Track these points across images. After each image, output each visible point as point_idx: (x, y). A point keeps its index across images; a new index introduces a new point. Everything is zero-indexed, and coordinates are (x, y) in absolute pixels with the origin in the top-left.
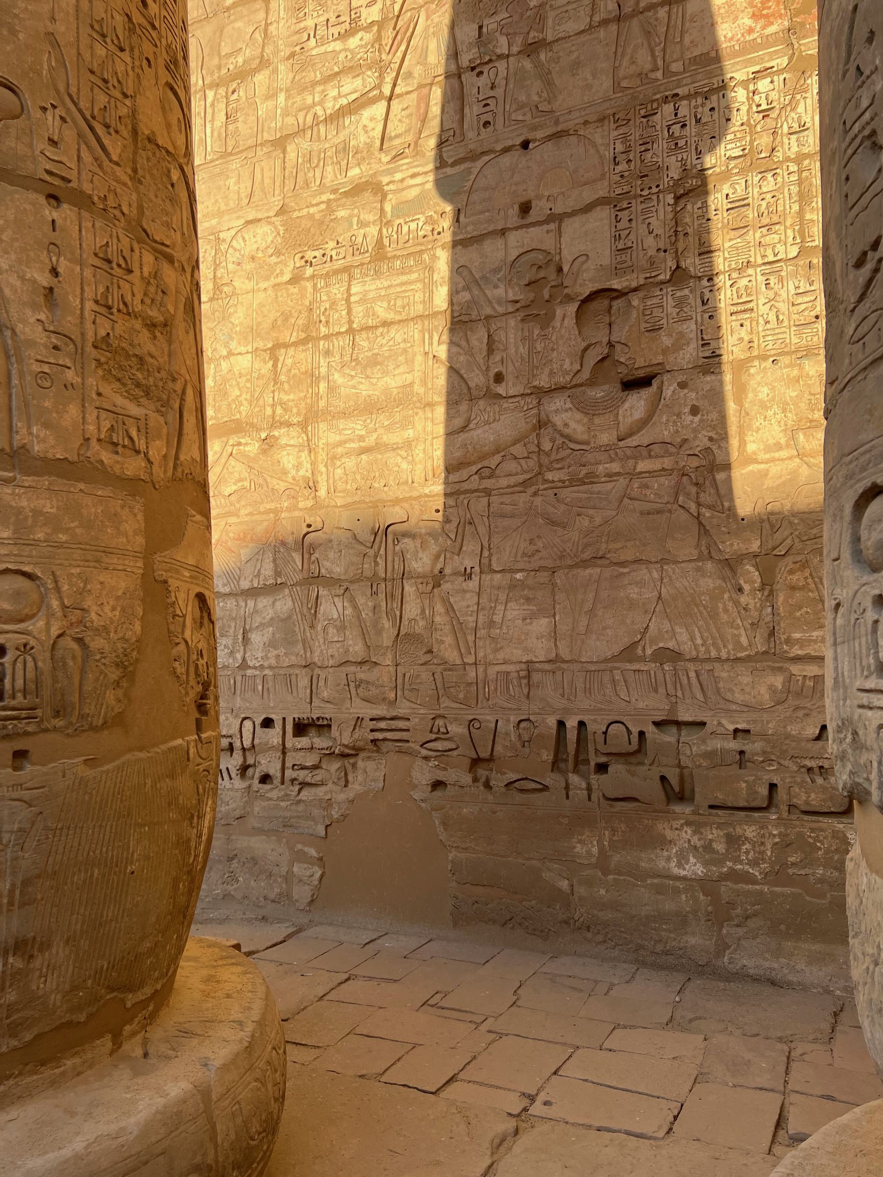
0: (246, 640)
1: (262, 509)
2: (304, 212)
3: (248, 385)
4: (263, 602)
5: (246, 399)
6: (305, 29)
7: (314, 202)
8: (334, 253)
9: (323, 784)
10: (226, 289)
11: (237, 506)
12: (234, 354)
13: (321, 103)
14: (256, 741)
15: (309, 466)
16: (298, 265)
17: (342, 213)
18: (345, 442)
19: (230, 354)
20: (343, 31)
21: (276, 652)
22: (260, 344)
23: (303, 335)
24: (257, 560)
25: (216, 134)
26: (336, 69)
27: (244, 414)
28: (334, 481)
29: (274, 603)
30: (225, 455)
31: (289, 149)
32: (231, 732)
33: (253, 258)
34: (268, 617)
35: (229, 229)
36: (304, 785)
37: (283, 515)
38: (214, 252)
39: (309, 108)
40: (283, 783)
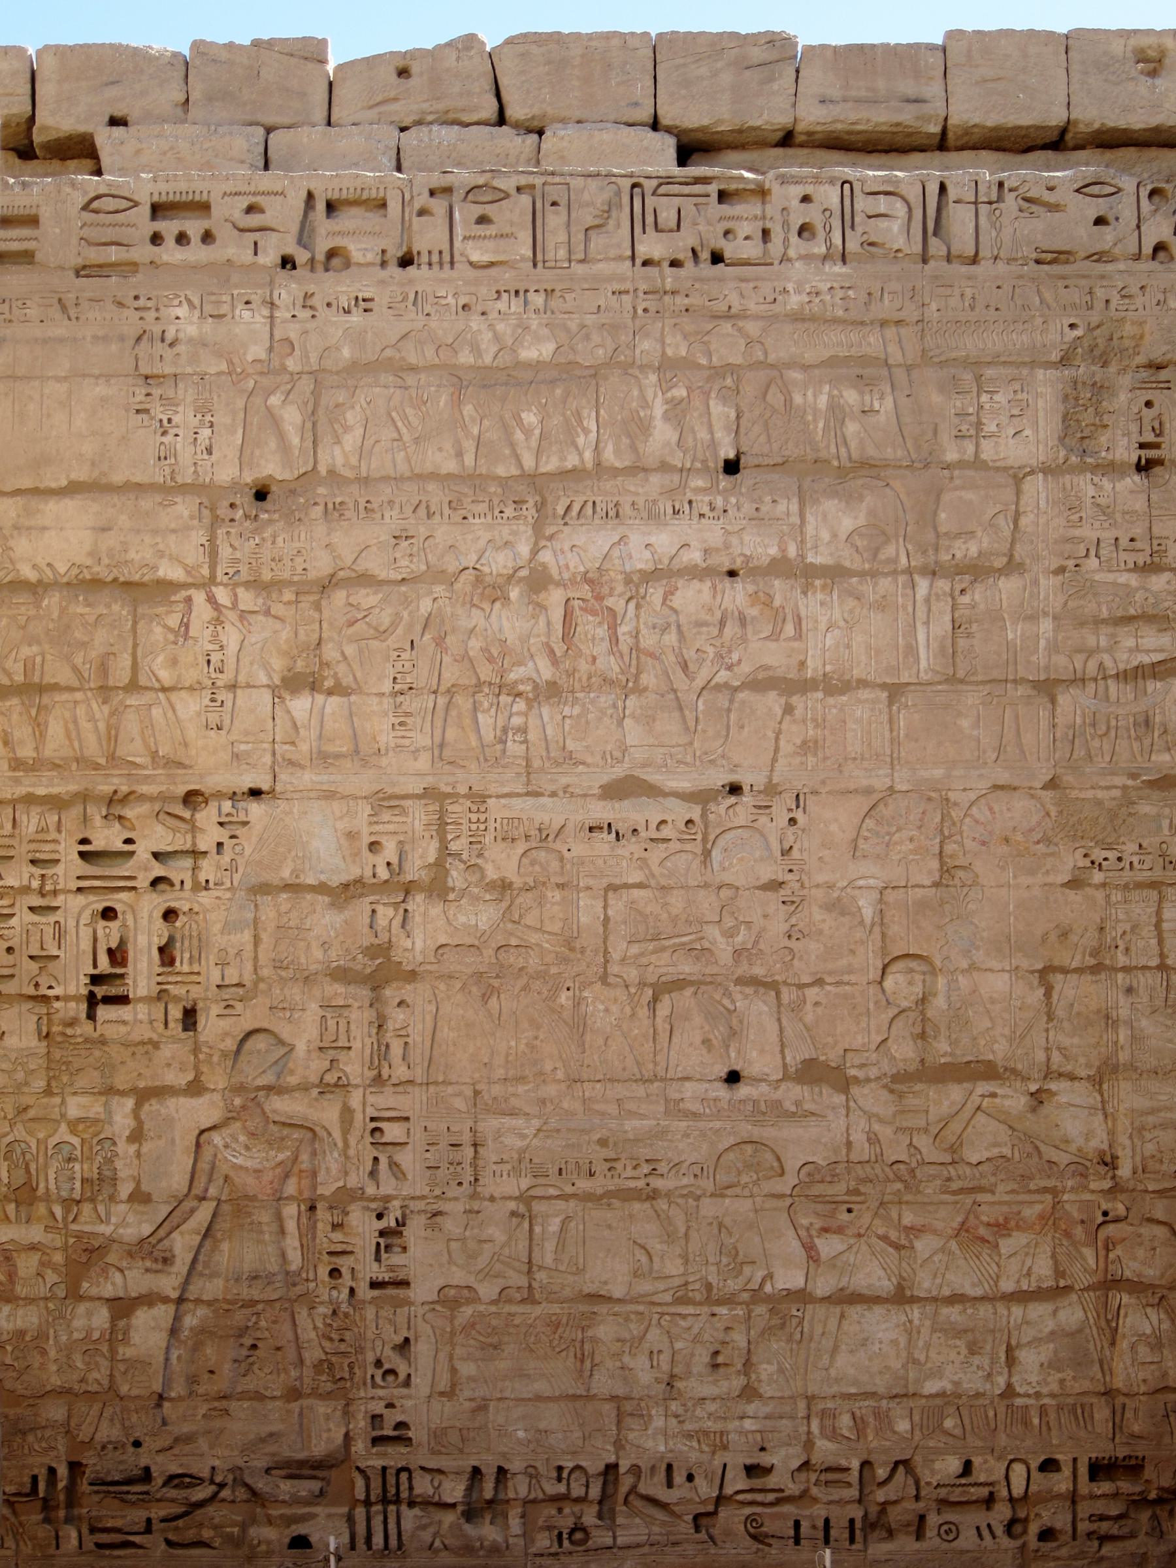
0: (1011, 1361)
1: (1032, 1186)
2: (1090, 794)
3: (1006, 1016)
4: (1038, 1310)
5: (1003, 1035)
6: (1081, 540)
7: (1102, 784)
8: (1135, 859)
9: (1132, 1536)
10: (961, 874)
11: (993, 1180)
12: (979, 969)
13: (1110, 650)
14: (1033, 1488)
15: (1105, 1136)
16: (1081, 864)
17: (1145, 808)
18: (1159, 1110)
19: (973, 968)
20: (1141, 563)
21: (1060, 1375)
22: (1025, 964)
23: (1093, 962)
24: (1027, 1254)
25: (934, 645)
26: (1132, 612)
27: (1000, 1055)
28: (1143, 1159)
29: (1055, 1312)
30: (970, 1107)
31: (1060, 699)
32: (992, 1479)
33: (1007, 840)
34: (1047, 1330)
35: (965, 790)
36: (1104, 1539)
37: (1065, 1197)
38: (938, 819)
39: (1091, 653)
40: (1074, 1538)
